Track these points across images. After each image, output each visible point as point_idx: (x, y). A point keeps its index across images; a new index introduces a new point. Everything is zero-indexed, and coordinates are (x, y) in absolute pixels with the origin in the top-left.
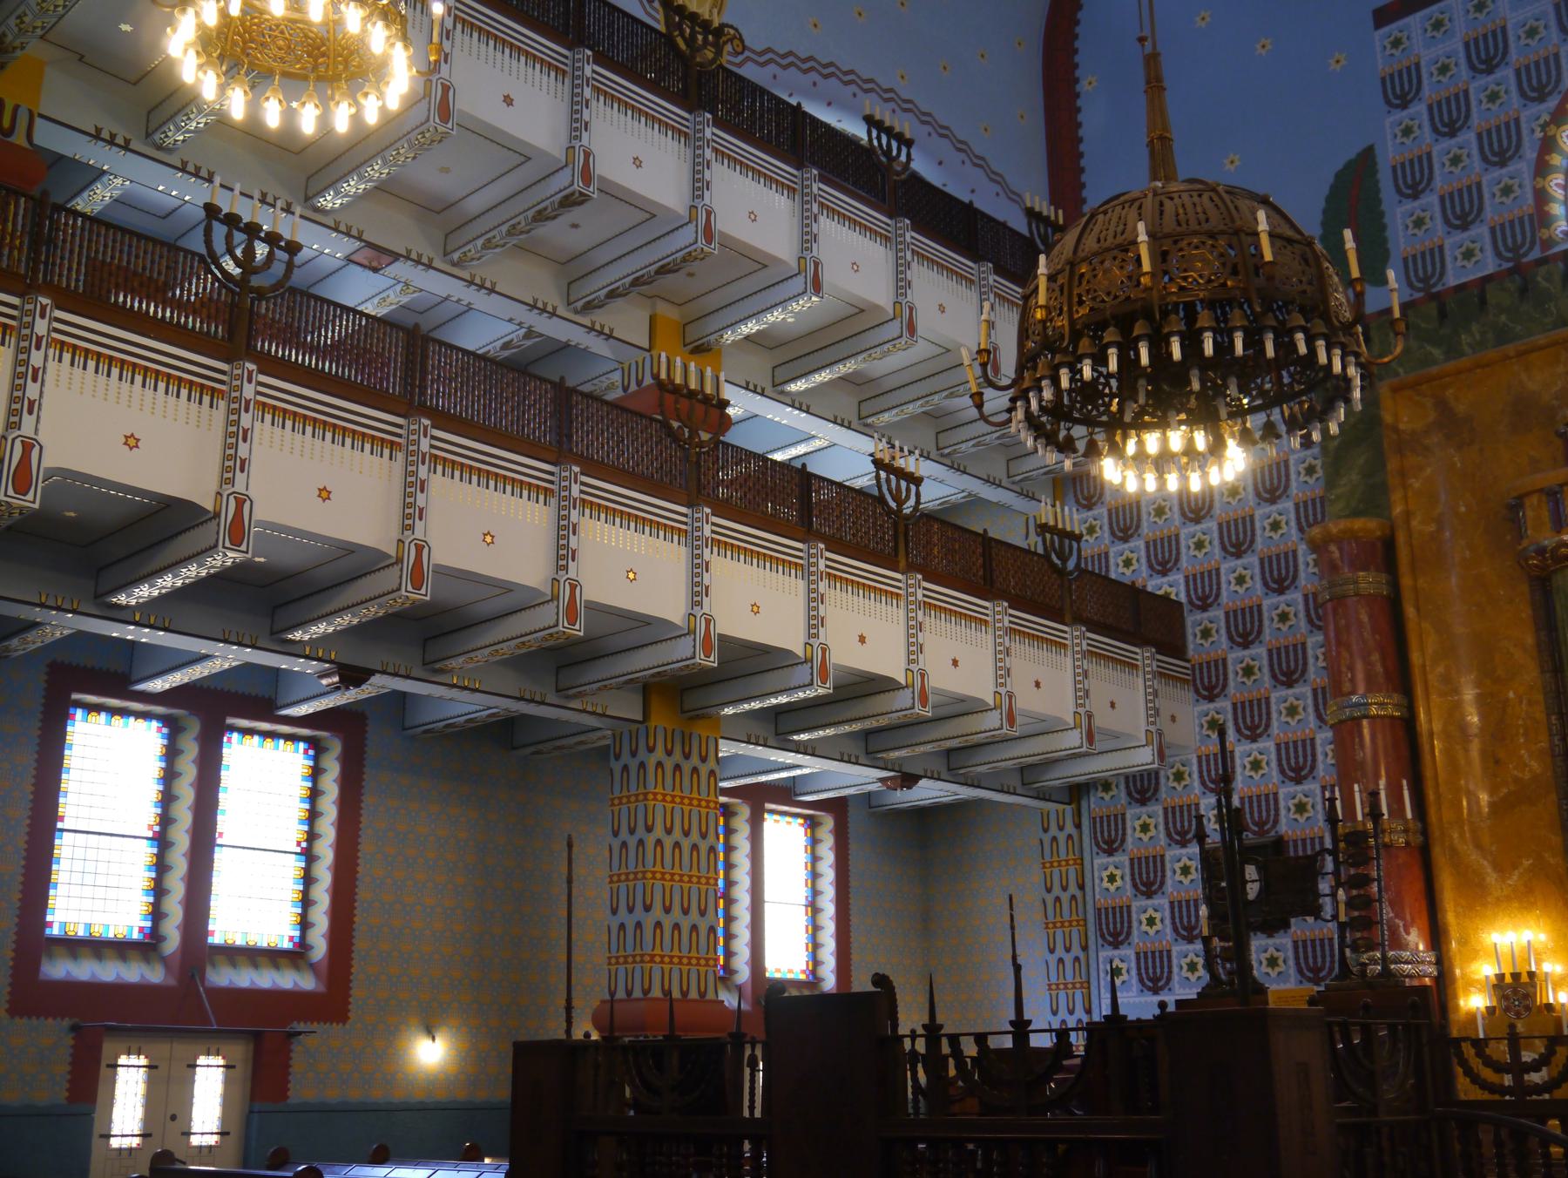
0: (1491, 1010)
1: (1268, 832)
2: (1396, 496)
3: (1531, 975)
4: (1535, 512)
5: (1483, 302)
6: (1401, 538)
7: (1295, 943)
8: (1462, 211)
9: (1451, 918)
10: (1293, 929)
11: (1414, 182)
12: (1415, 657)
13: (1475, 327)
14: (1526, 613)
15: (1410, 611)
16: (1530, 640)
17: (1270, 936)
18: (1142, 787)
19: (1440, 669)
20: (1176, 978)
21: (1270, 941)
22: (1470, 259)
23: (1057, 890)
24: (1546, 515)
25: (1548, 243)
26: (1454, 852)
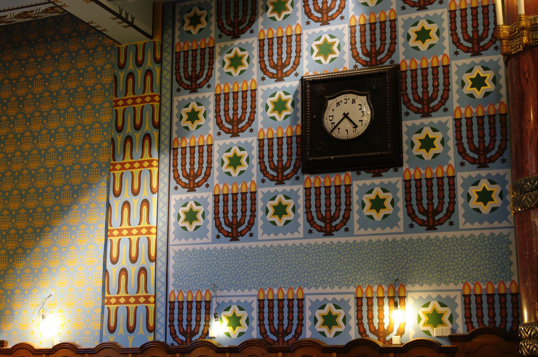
1: (382, 62)
7: (407, 184)
10: (406, 166)
17: (377, 175)
21: (377, 181)
23: (129, 129)
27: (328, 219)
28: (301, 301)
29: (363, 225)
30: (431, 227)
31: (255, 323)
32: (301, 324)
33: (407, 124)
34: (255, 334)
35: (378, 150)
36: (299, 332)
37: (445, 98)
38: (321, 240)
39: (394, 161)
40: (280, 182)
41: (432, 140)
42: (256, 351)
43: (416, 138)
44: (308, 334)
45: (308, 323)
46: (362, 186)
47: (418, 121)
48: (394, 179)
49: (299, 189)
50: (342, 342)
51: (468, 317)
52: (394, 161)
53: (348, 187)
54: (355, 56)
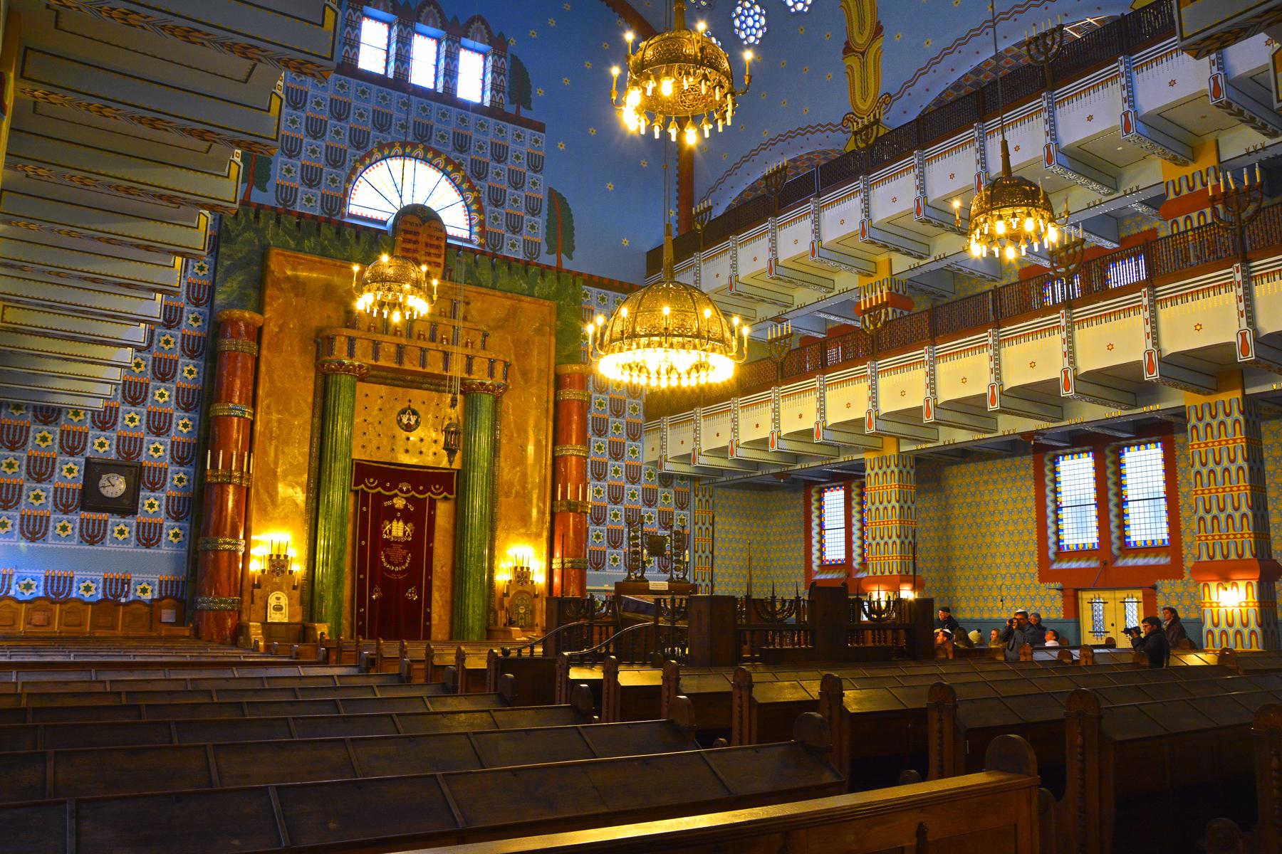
0: (263, 571)
2: (268, 308)
3: (286, 556)
4: (340, 345)
5: (318, 229)
6: (266, 330)
7: (138, 524)
8: (311, 177)
9: (253, 525)
11: (292, 150)
12: (261, 392)
13: (312, 239)
14: (311, 386)
15: (263, 368)
16: (310, 400)
18: (49, 415)
19: (266, 402)
20: (50, 534)
22: (308, 203)
24: (346, 348)
25: (343, 216)
26: (257, 493)
27: (93, 536)
28: (72, 579)
29: (112, 542)
30: (148, 547)
31: (41, 588)
32: (70, 590)
33: (142, 494)
34: (41, 594)
35: (126, 506)
36: (69, 594)
37: (163, 485)
38: (87, 547)
39: (135, 513)
40: (66, 513)
41: (153, 504)
42: (43, 602)
43: (147, 502)
44: (74, 595)
45: (75, 589)
46: (115, 523)
47: (148, 494)
48: (132, 521)
49: (77, 519)
50: (94, 600)
51: (160, 591)
52: (135, 513)
53: (106, 522)
54: (118, 452)
